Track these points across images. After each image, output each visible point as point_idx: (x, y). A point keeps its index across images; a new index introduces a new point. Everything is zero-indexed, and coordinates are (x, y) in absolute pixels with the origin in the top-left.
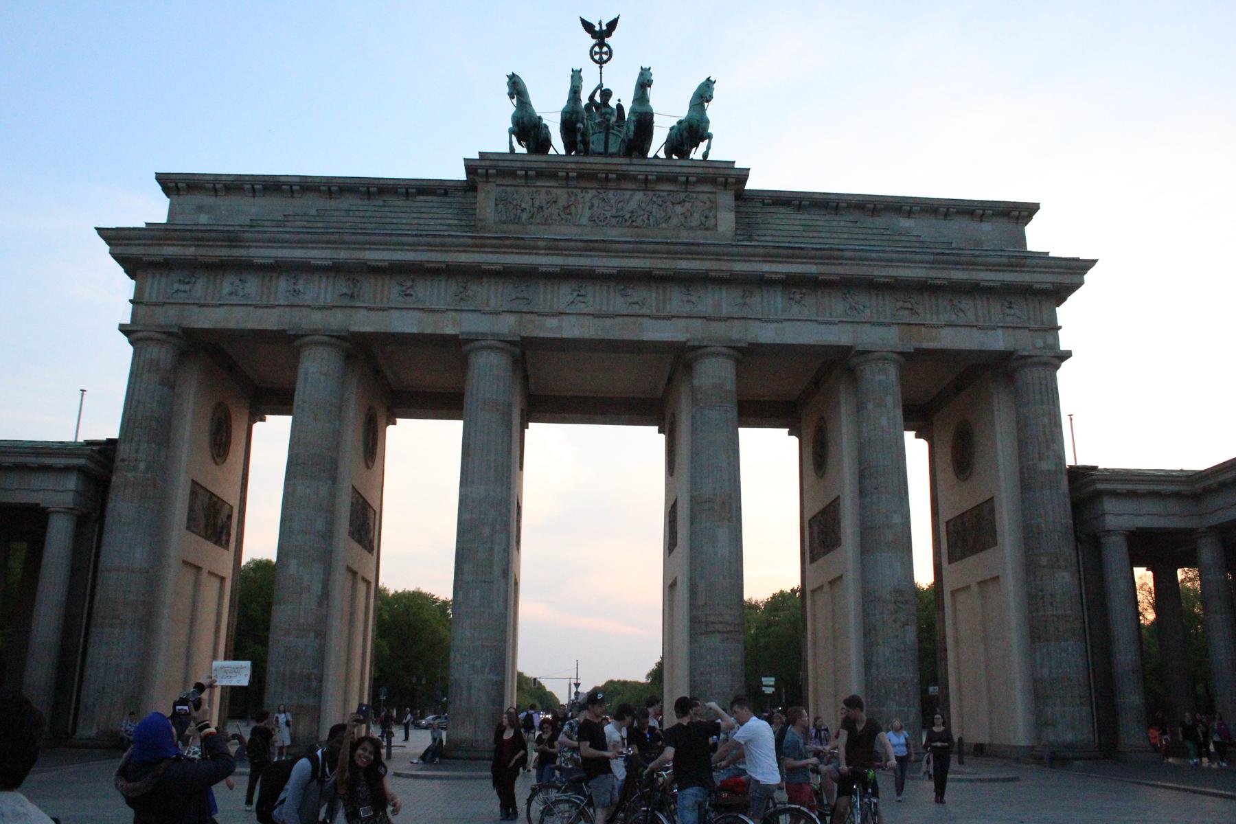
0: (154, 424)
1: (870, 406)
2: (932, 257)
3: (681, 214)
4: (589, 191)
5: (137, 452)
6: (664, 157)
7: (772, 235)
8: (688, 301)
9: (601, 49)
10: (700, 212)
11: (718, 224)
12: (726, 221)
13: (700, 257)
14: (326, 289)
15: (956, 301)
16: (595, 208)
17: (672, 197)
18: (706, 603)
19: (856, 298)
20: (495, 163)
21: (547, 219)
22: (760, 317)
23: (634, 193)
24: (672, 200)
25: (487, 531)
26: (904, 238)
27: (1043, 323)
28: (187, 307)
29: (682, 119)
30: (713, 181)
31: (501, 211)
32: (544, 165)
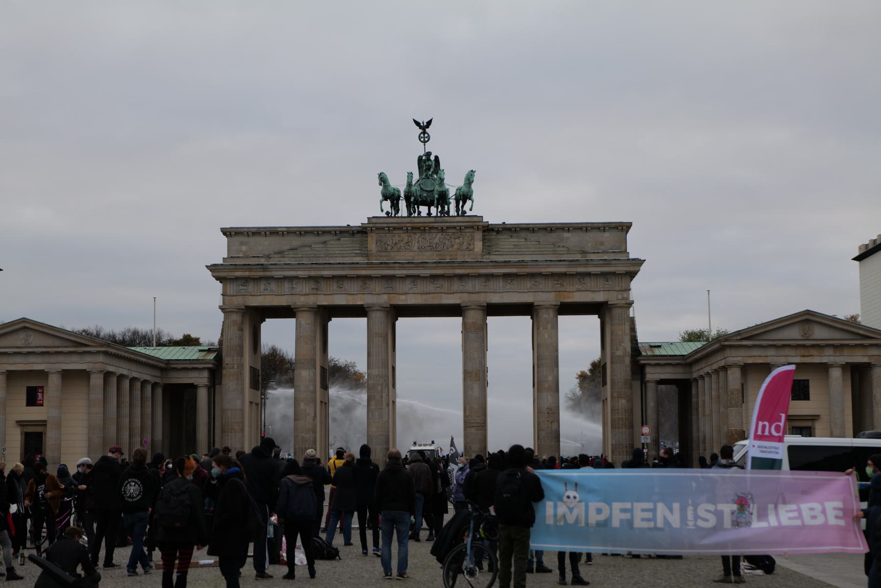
0: (238, 348)
1: (541, 329)
2: (567, 263)
4: (418, 234)
5: (233, 360)
7: (498, 251)
8: (462, 285)
9: (424, 135)
12: (478, 246)
14: (306, 287)
15: (581, 280)
18: (469, 416)
19: (535, 280)
21: (398, 249)
22: (492, 291)
25: (379, 388)
26: (562, 249)
27: (622, 287)
28: (246, 296)
30: (472, 227)
32: (396, 225)
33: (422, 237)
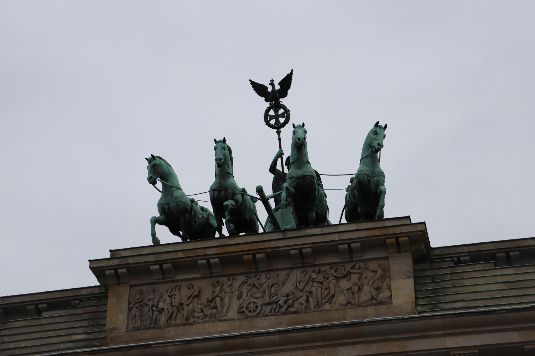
3: (347, 290)
4: (237, 277)
6: (346, 222)
7: (462, 301)
9: (276, 111)
10: (370, 284)
11: (393, 297)
13: (364, 339)
16: (244, 297)
17: (336, 271)
20: (123, 261)
21: (187, 319)
23: (291, 271)
24: (335, 275)
29: (354, 176)
31: (135, 315)
32: (180, 255)
33: (250, 281)
